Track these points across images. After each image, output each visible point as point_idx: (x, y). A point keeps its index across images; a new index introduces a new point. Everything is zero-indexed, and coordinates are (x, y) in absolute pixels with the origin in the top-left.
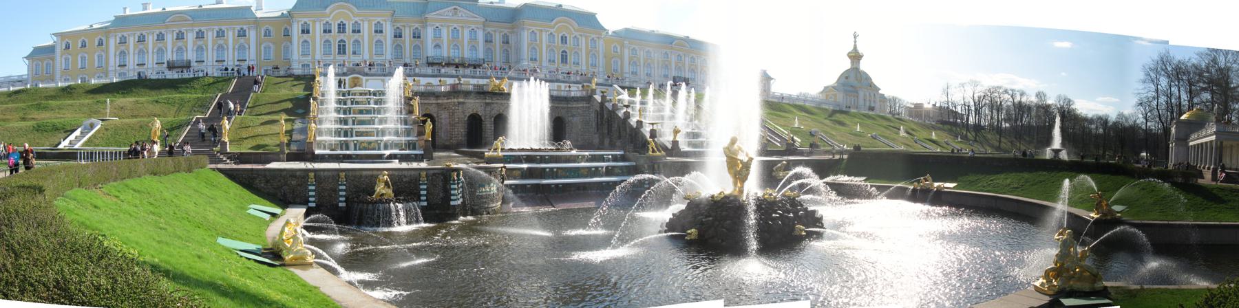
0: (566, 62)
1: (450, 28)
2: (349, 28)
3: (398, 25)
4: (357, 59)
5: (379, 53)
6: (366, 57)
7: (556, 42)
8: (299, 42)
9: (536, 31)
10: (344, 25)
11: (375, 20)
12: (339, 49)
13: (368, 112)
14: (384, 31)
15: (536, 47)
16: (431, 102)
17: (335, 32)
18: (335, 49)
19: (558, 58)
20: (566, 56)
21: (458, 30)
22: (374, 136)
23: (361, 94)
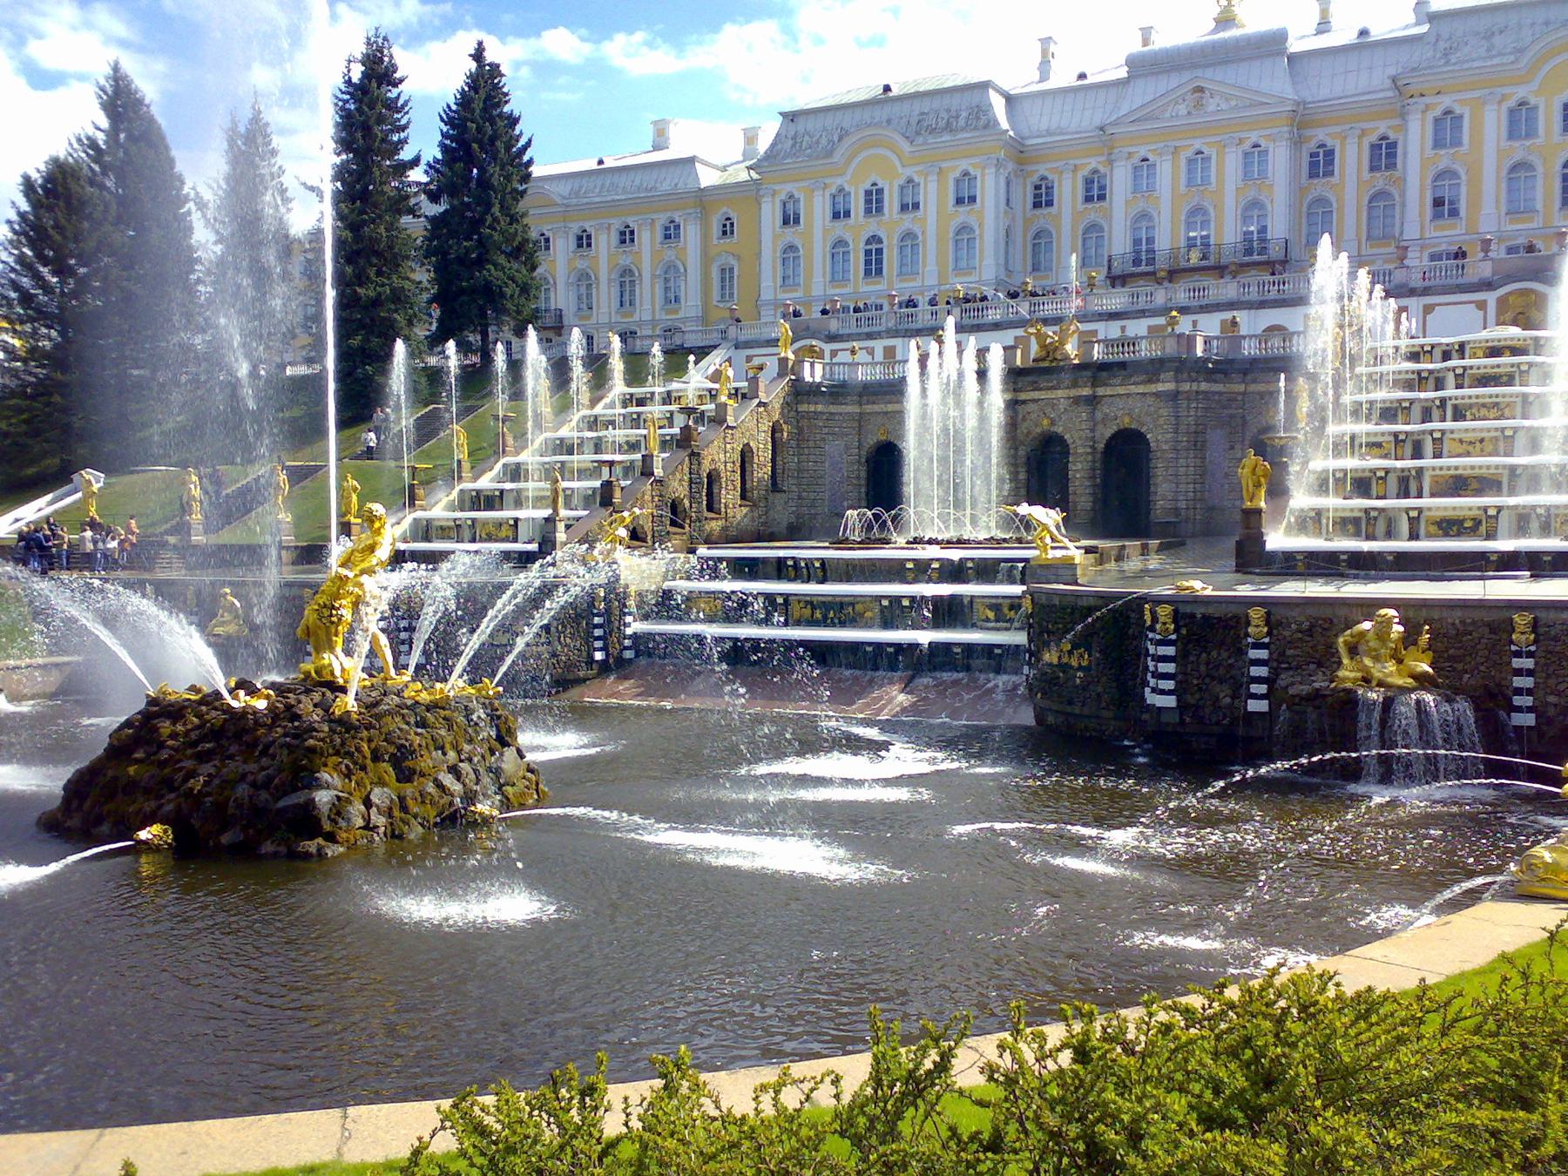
2: (891, 202)
6: (931, 280)
8: (775, 252)
10: (880, 192)
12: (868, 262)
14: (978, 200)
17: (857, 214)
18: (857, 260)
21: (1209, 159)
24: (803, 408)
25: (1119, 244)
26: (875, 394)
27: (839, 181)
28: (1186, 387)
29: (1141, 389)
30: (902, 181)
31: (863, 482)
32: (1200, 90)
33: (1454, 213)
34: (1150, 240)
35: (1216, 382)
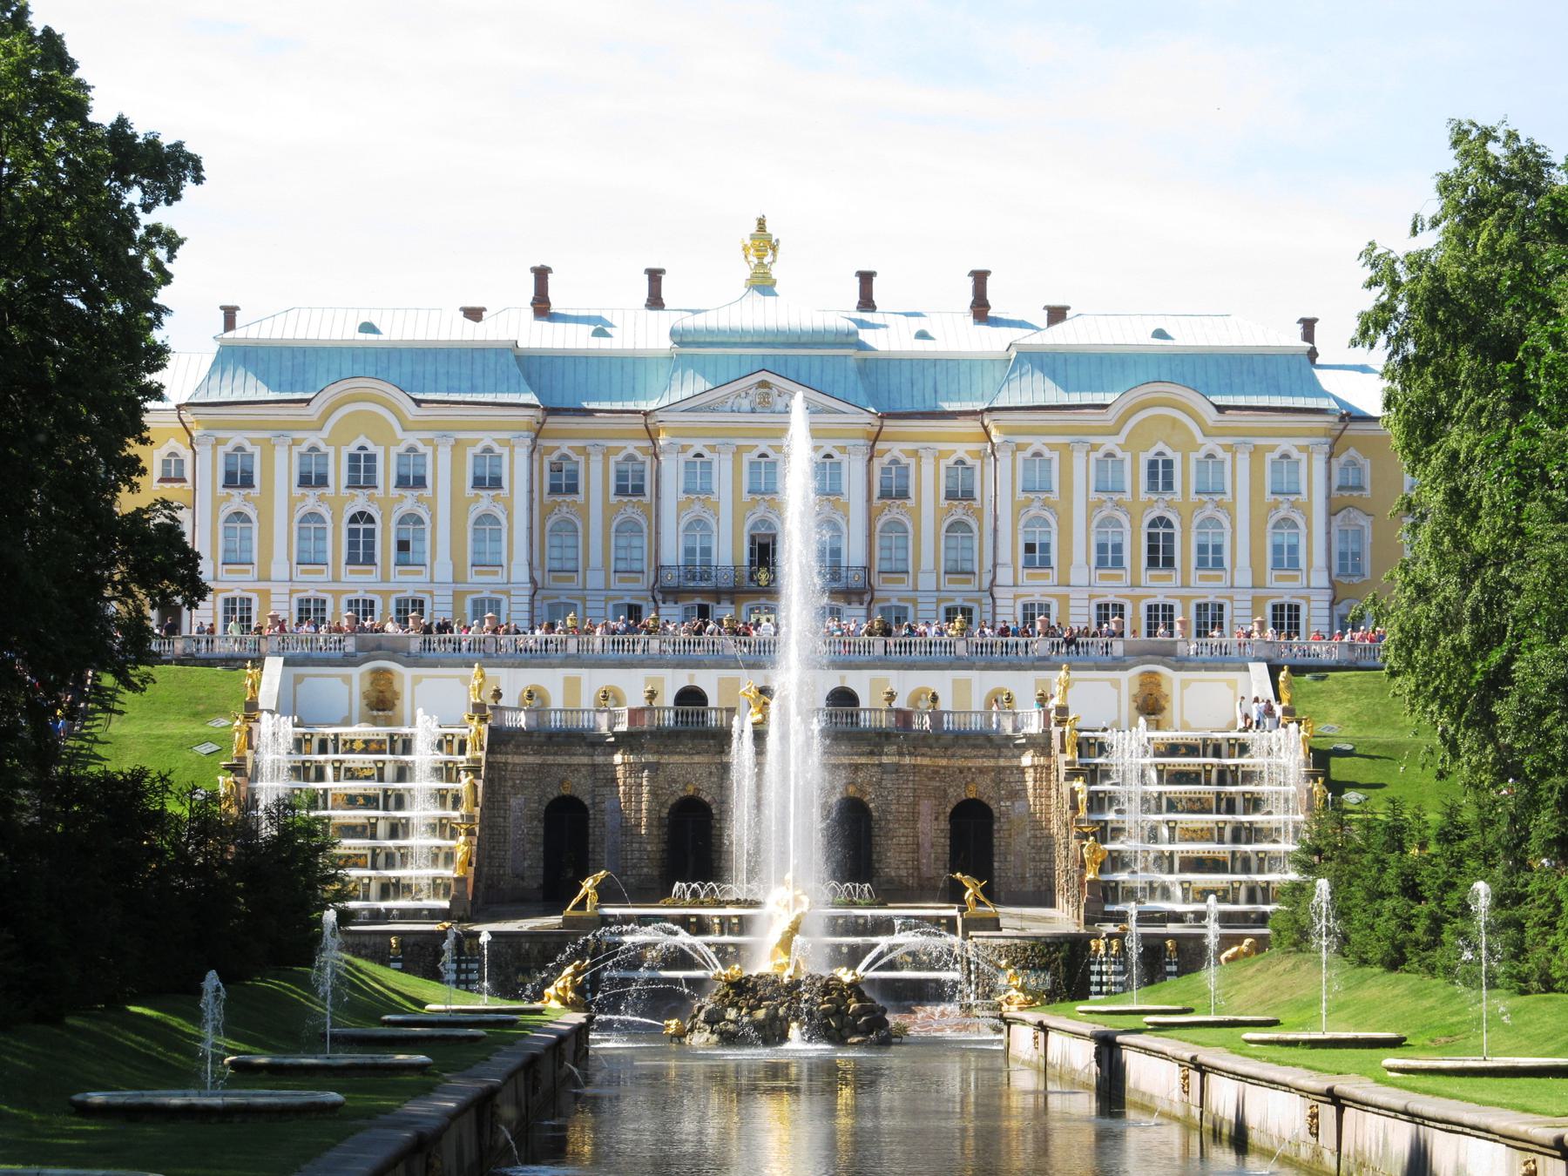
0: (1169, 562)
1: (747, 458)
2: (386, 473)
3: (565, 450)
4: (408, 584)
5: (488, 559)
7: (1128, 486)
9: (1047, 454)
10: (371, 458)
11: (474, 443)
12: (353, 545)
13: (370, 801)
14: (505, 483)
15: (1046, 514)
16: (576, 760)
18: (336, 542)
19: (1135, 549)
20: (1169, 538)
22: (364, 867)
23: (368, 747)
24: (501, 758)
25: (672, 553)
26: (558, 745)
27: (312, 438)
28: (907, 760)
29: (863, 760)
30: (402, 449)
31: (540, 840)
32: (764, 384)
33: (1046, 563)
34: (706, 551)
35: (923, 755)
